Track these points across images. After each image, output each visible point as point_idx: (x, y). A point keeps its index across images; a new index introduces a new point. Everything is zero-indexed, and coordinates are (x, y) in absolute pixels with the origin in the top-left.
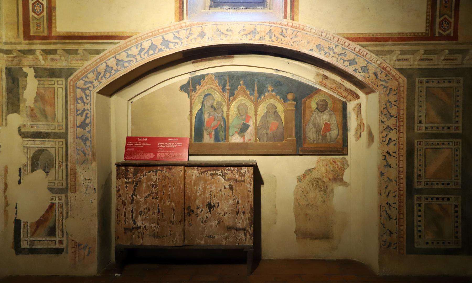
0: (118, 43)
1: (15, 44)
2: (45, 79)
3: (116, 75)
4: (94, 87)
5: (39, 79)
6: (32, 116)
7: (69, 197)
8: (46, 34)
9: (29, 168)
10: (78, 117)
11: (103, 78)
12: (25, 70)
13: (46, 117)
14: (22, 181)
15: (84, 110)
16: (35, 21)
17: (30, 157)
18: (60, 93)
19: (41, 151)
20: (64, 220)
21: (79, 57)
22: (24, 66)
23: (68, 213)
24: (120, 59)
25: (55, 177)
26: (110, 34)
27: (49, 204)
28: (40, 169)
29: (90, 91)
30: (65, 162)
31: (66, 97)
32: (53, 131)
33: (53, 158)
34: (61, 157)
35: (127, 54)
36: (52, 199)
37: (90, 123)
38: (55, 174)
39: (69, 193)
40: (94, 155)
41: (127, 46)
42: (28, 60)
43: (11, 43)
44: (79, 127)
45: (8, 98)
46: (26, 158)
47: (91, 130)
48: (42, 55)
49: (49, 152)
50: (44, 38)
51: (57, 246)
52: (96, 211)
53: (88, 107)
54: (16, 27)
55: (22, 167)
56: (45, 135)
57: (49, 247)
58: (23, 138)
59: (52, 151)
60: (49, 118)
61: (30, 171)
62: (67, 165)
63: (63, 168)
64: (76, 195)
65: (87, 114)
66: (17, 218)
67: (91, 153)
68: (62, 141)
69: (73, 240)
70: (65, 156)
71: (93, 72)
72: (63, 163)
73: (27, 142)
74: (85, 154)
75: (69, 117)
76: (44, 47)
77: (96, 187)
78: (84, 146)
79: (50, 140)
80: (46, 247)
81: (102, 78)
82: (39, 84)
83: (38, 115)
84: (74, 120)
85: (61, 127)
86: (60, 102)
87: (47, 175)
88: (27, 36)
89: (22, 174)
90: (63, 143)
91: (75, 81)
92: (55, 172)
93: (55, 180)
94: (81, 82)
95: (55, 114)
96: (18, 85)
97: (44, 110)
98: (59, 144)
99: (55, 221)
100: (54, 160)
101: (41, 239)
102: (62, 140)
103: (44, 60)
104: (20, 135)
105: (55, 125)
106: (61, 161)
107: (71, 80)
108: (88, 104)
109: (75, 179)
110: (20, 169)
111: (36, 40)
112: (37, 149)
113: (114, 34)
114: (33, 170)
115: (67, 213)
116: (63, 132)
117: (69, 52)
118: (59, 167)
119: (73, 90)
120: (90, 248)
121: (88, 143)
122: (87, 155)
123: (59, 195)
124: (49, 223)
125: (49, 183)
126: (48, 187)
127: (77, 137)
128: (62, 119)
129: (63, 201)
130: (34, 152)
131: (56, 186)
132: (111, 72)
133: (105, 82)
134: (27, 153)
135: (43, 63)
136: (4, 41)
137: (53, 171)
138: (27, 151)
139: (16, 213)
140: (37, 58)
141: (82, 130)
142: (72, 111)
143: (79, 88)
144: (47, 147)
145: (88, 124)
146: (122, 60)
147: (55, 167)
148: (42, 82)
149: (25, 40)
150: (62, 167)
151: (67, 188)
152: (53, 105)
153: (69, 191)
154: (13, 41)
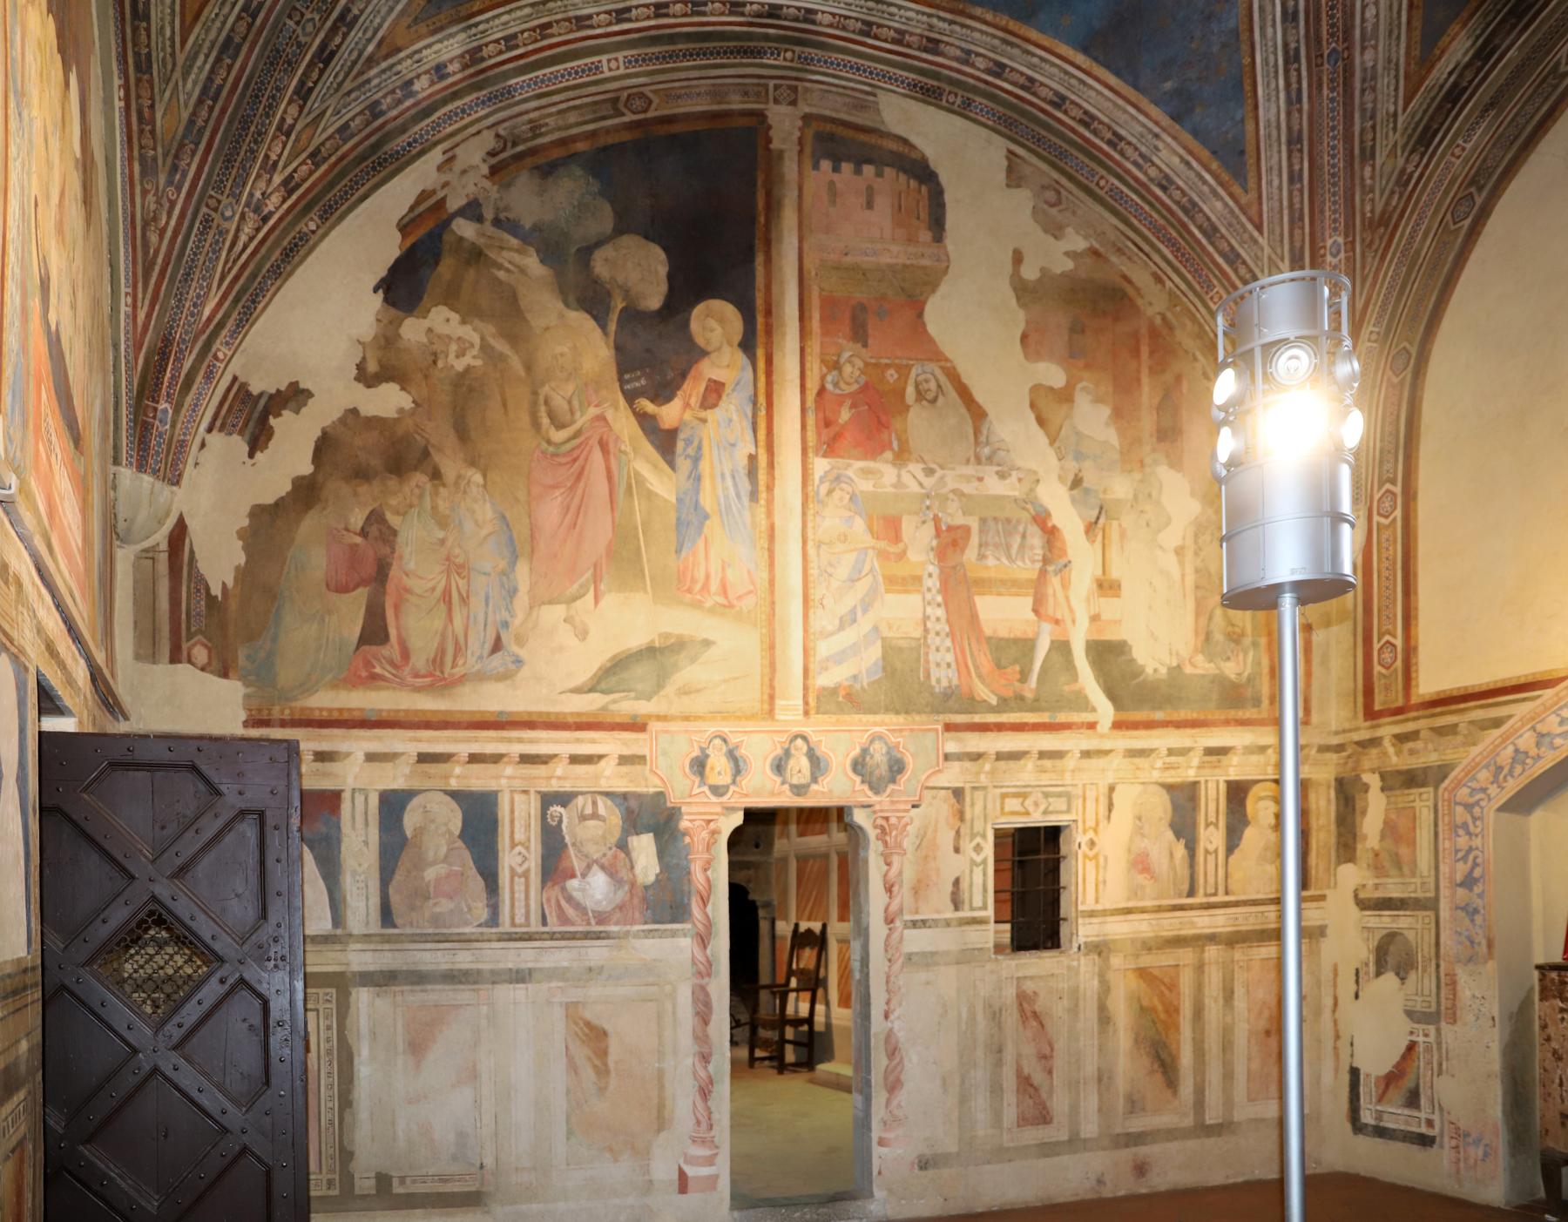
0: (1539, 696)
1: (1350, 731)
2: (1398, 792)
3: (1535, 768)
4: (1489, 800)
5: (1389, 793)
6: (1378, 868)
7: (1443, 1032)
8: (1400, 702)
9: (1372, 968)
11: (1509, 778)
12: (1366, 778)
13: (1400, 869)
15: (1470, 849)
16: (1383, 681)
18: (1426, 816)
19: (1391, 937)
21: (1459, 738)
22: (1364, 771)
24: (1545, 732)
26: (1523, 681)
27: (1406, 1043)
29: (1482, 808)
31: (1436, 825)
32: (1413, 895)
34: (1425, 949)
35: (1558, 719)
36: (1412, 1033)
37: (1482, 876)
39: (1443, 1025)
40: (1490, 945)
41: (1560, 699)
42: (1371, 758)
43: (1344, 731)
44: (1461, 885)
45: (1340, 835)
48: (1393, 745)
50: (1399, 711)
51: (1424, 1130)
52: (1497, 1067)
53: (1477, 842)
54: (1352, 699)
59: (1410, 935)
60: (1406, 870)
62: (1438, 966)
64: (1456, 1028)
65: (1476, 858)
67: (1484, 942)
71: (1487, 766)
74: (1472, 942)
76: (1398, 729)
77: (1496, 1014)
79: (1408, 913)
81: (1505, 777)
82: (1388, 804)
83: (1387, 864)
86: (1424, 837)
88: (1371, 714)
91: (1454, 789)
94: (1465, 791)
96: (1354, 809)
97: (1397, 854)
99: (1418, 1078)
102: (1428, 913)
103: (1398, 753)
104: (1357, 904)
107: (1446, 789)
108: (1477, 836)
109: (1455, 995)
110: (1357, 970)
111: (1385, 716)
113: (1530, 679)
114: (1378, 974)
115: (1440, 1065)
117: (1440, 731)
118: (1424, 970)
119: (1449, 809)
121: (1478, 919)
123: (1424, 1026)
124: (1408, 1083)
127: (1457, 908)
129: (1432, 1039)
131: (1418, 1008)
132: (1524, 763)
133: (1512, 786)
135: (1396, 760)
136: (1334, 728)
137: (1412, 977)
139: (1352, 1056)
140: (1385, 754)
143: (1460, 804)
145: (1476, 881)
146: (1548, 734)
148: (1392, 799)
149: (1366, 720)
151: (1438, 1012)
152: (1412, 843)
154: (1347, 726)
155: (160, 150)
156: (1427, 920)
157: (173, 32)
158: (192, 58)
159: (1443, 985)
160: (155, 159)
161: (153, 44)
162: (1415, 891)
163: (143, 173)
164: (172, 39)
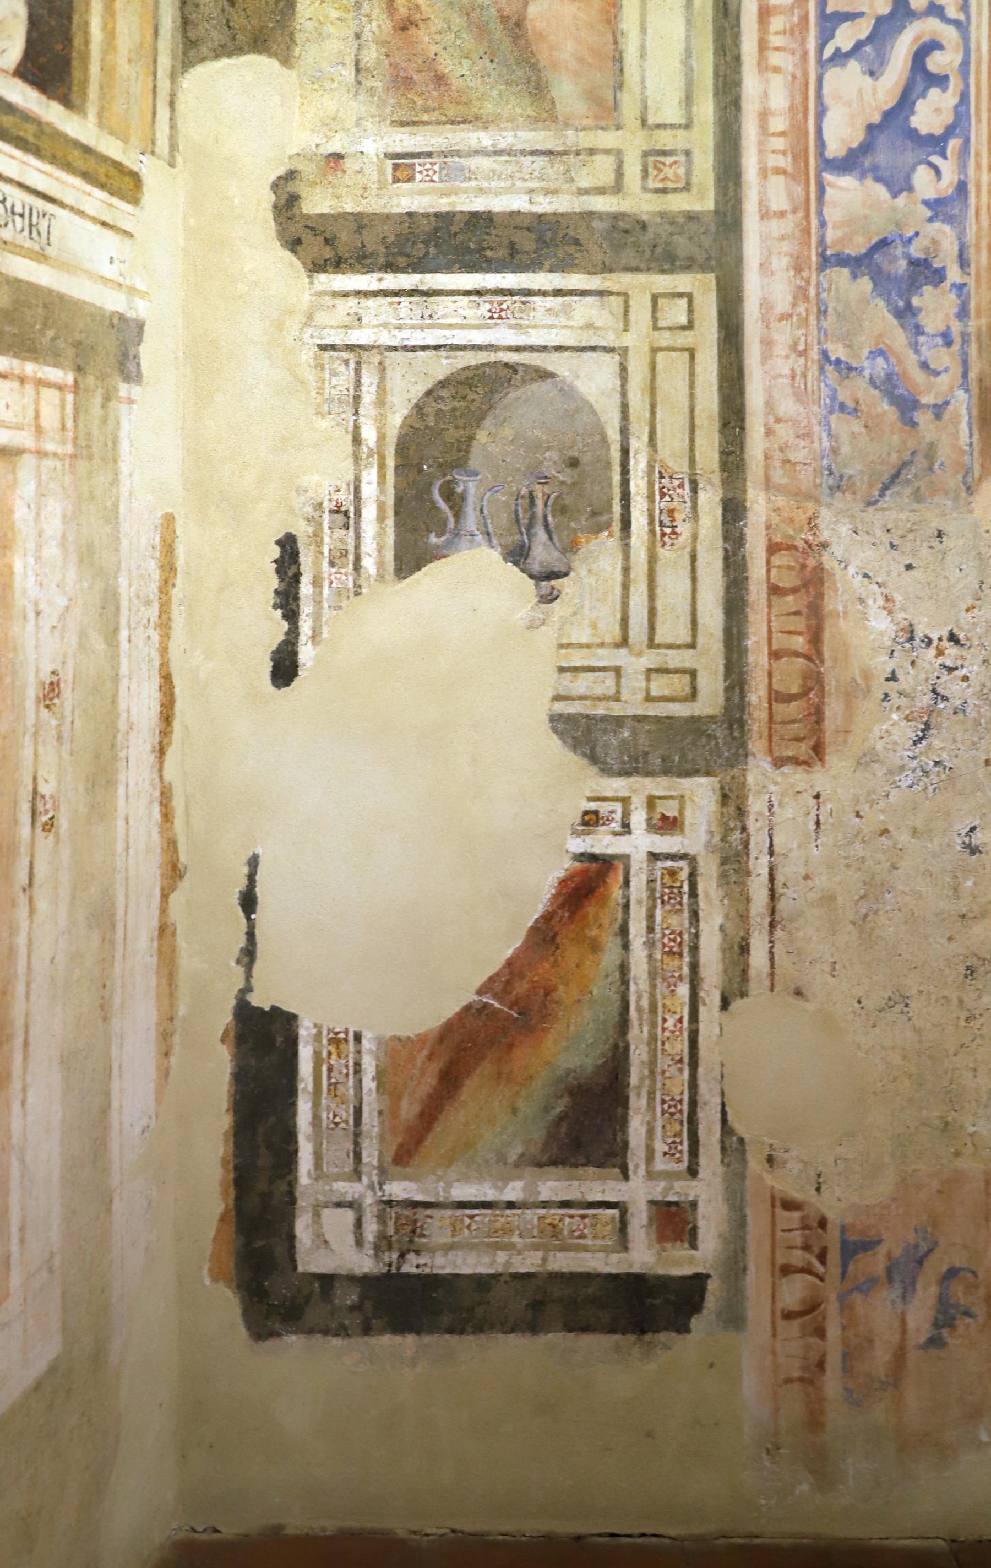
7: (756, 805)
10: (833, 76)
14: (306, 653)
17: (381, 438)
20: (709, 1013)
23: (744, 949)
25: (625, 621)
27: (561, 868)
28: (472, 544)
30: (717, 478)
33: (604, 439)
36: (591, 820)
38: (626, 587)
46: (350, 448)
47: (962, 188)
49: (568, 392)
55: (302, 530)
56: (527, 242)
57: (562, 1262)
58: (317, 267)
61: (381, 565)
63: (695, 537)
64: (819, 779)
66: (259, 1000)
68: (690, 297)
69: (789, 1205)
70: (716, 425)
72: (694, 490)
73: (352, 301)
75: (751, 84)
78: (899, 338)
79: (576, 280)
80: (528, 1263)
84: (798, 110)
85: (674, 171)
87: (550, 598)
89: (305, 588)
90: (690, 311)
92: (626, 570)
93: (624, 642)
95: (618, 59)
98: (655, 319)
99: (623, 1024)
100: (608, 465)
101: (489, 1194)
102: (683, 281)
105: (618, 154)
106: (680, 467)
109: (816, 638)
112: (444, 366)
116: (691, 217)
120: (952, 1273)
122: (923, 418)
125: (562, 670)
126: (560, 707)
128: (689, 100)
130: (419, 390)
131: (632, 704)
134: (357, 399)
138: (358, 385)
141: (881, 191)
142: (777, 23)
144: (544, 349)
147: (616, 526)
150: (684, 529)
153: (757, 745)
156: (676, 313)
159: (757, 592)
162: (617, 187)
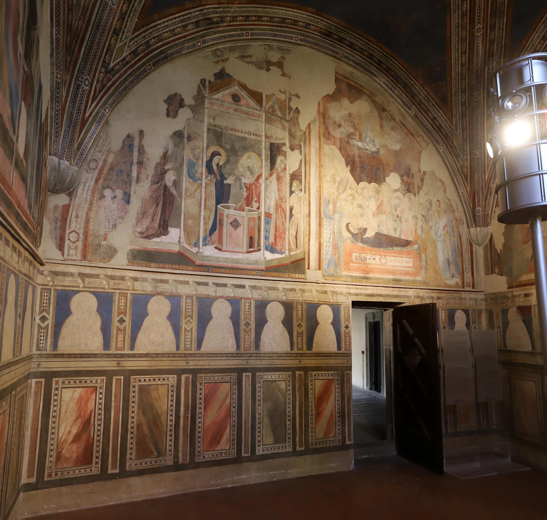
155: (458, 150)
157: (449, 124)
158: (456, 125)
160: (458, 153)
161: (446, 130)
163: (457, 158)
164: (450, 126)
